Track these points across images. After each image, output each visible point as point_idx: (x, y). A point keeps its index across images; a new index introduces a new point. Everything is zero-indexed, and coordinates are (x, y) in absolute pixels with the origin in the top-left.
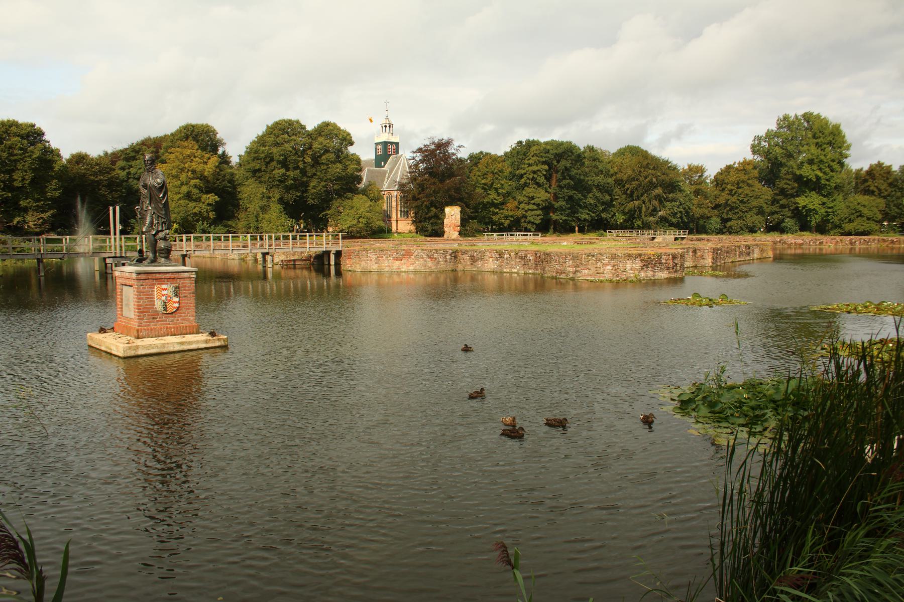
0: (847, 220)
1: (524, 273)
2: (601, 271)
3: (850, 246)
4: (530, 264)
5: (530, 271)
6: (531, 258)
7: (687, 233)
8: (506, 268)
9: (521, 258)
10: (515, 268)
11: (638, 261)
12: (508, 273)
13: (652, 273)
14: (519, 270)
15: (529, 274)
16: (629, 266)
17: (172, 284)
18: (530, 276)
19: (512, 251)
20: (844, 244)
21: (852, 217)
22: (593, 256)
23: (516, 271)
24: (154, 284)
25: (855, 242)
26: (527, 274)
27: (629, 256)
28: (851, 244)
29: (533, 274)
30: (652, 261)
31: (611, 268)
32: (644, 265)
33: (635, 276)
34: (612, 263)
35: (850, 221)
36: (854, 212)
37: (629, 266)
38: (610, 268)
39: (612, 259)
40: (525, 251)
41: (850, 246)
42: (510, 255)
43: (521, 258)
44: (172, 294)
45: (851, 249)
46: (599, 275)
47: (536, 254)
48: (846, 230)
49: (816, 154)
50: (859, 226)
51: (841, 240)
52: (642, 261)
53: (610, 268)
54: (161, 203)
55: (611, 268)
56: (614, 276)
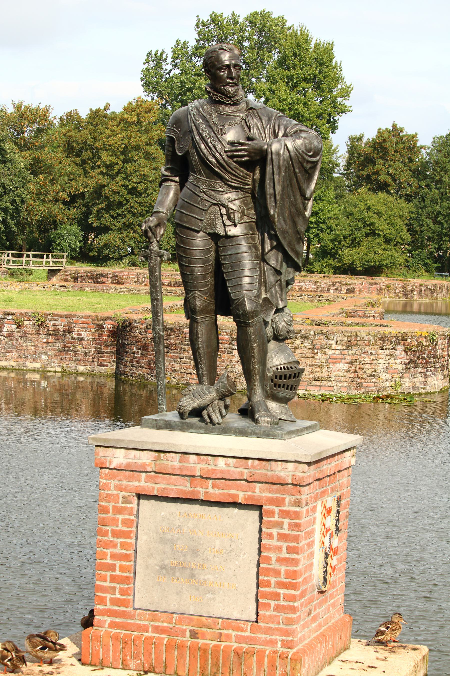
0: (348, 240)
1: (63, 373)
2: (324, 374)
3: (403, 300)
4: (80, 350)
5: (81, 368)
6: (85, 335)
7: (64, 260)
8: (6, 359)
9: (55, 334)
10: (34, 359)
11: (399, 352)
12: (12, 369)
13: (422, 379)
14: (46, 364)
15: (78, 374)
16: (382, 364)
17: (333, 490)
18: (81, 379)
19: (28, 316)
20: (392, 294)
21: (358, 235)
22: (306, 338)
23: (37, 365)
24: (316, 499)
25: (412, 291)
26: (71, 373)
27: (384, 339)
28: (405, 294)
29: (88, 375)
30: (422, 352)
31: (346, 367)
32: (411, 362)
33: (395, 387)
34: (349, 355)
35: (354, 243)
36: (361, 225)
37: (382, 364)
38: (343, 366)
39: (349, 346)
40: (67, 316)
41: (403, 300)
42: (20, 326)
43: (55, 334)
44: (333, 528)
45: (406, 305)
46: (317, 383)
47: (101, 327)
48: (347, 261)
49: (290, 101)
50: (370, 256)
51: (387, 287)
52: (406, 350)
53: (343, 366)
54: (304, 216)
55: (346, 367)
56: (353, 386)
